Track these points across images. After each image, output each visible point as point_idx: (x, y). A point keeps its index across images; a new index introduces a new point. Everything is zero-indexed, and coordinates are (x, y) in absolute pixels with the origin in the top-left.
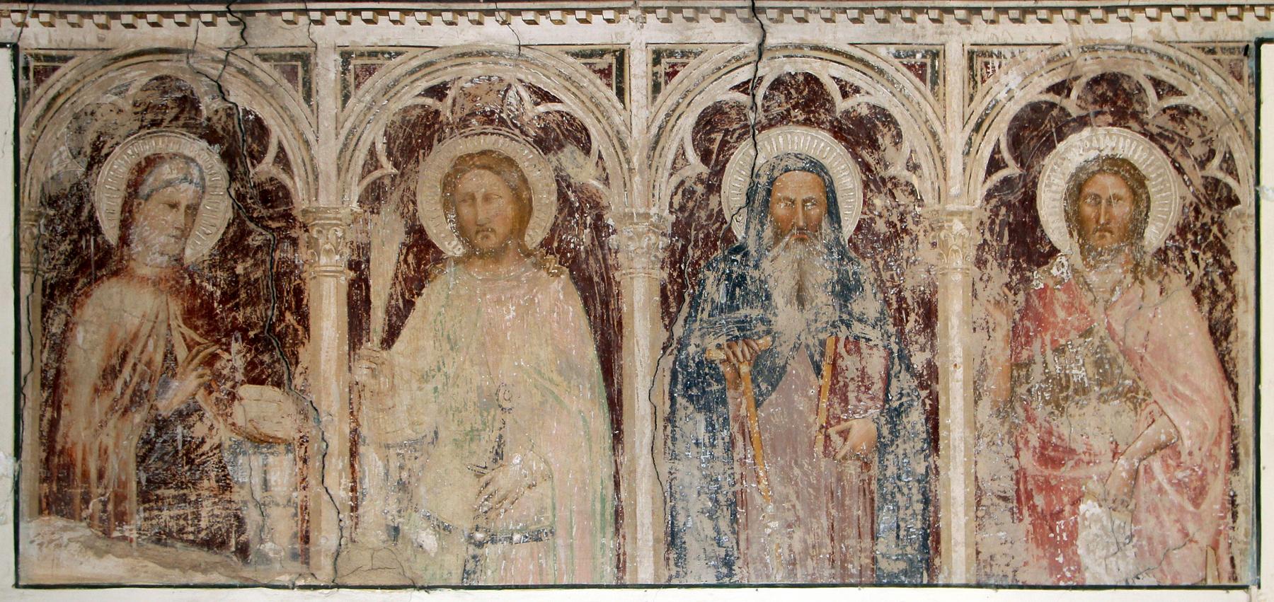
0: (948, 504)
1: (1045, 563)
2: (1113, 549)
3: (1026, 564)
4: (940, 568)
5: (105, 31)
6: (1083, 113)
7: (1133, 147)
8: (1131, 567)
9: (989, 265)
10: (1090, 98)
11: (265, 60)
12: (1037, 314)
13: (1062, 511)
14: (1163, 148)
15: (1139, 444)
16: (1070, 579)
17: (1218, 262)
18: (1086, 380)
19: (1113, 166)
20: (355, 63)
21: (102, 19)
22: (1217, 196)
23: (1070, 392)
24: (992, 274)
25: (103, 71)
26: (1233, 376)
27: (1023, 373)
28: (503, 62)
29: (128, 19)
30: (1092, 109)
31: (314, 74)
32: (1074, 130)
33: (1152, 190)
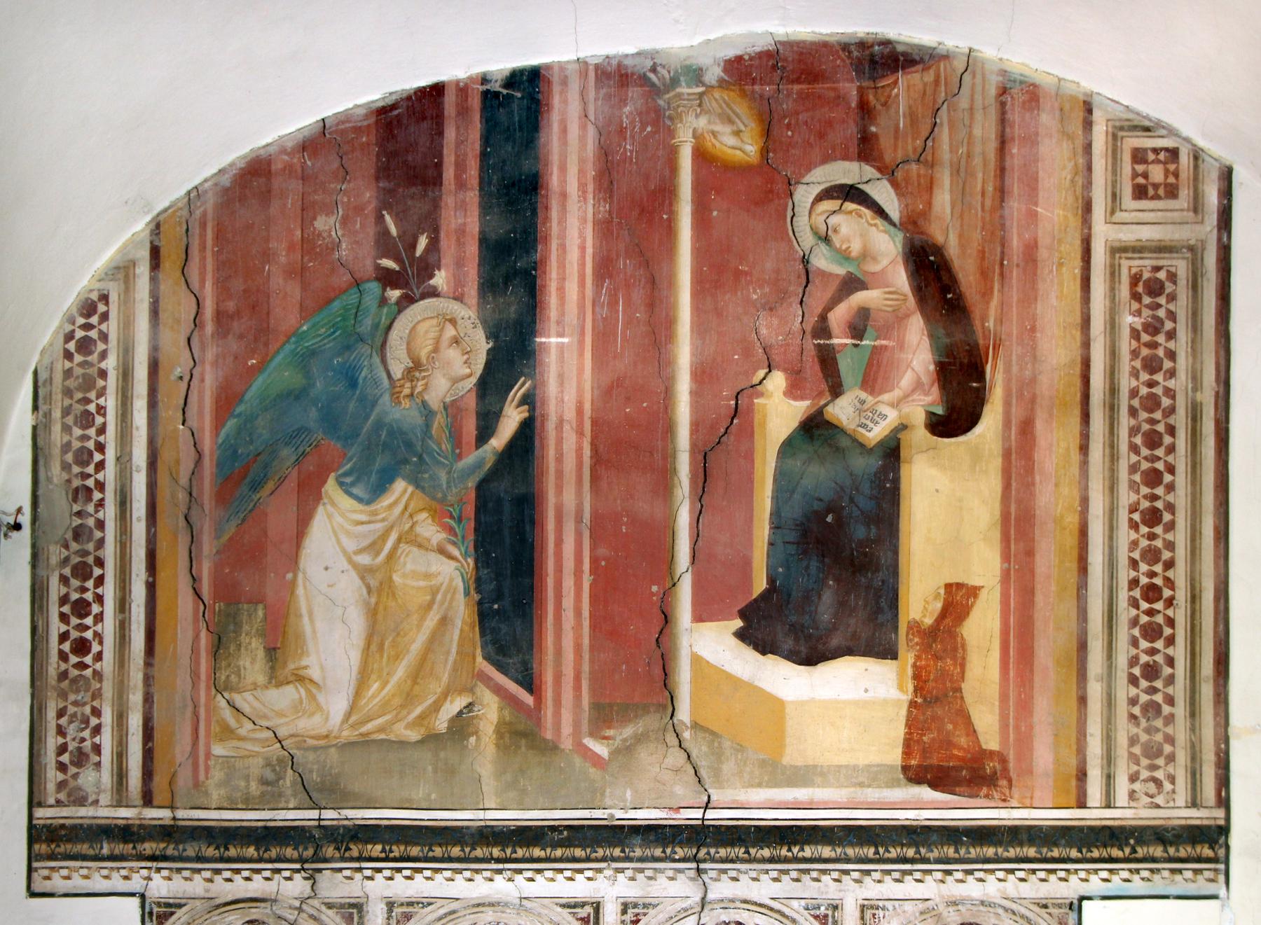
5: (210, 884)
11: (330, 908)
20: (398, 911)
21: (207, 874)
25: (207, 916)
28: (508, 911)
29: (227, 874)
31: (366, 920)
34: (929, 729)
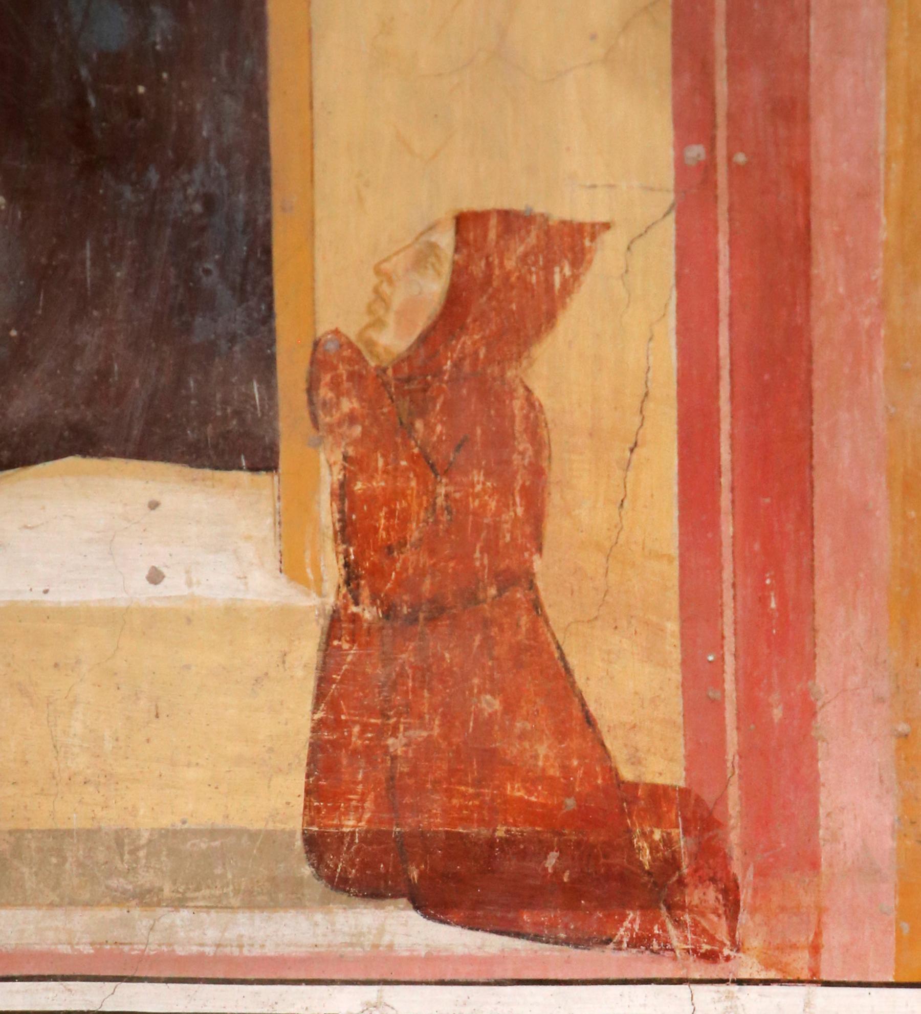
34: (409, 710)
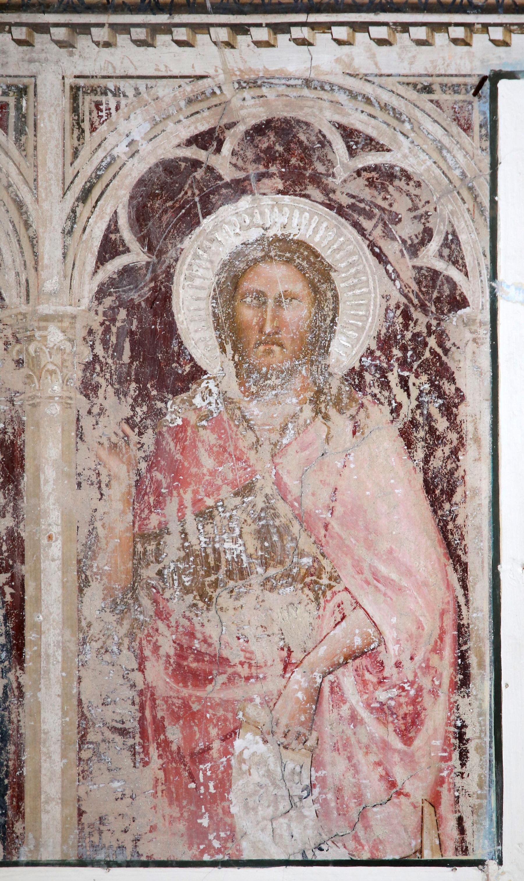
0: (37, 742)
1: (181, 827)
2: (283, 806)
3: (153, 829)
4: (22, 837)
6: (241, 175)
7: (313, 225)
8: (310, 832)
9: (101, 393)
10: (250, 154)
12: (172, 461)
13: (208, 749)
14: (356, 225)
15: (322, 650)
16: (219, 851)
17: (436, 388)
18: (244, 558)
19: (285, 251)
22: (435, 295)
23: (221, 575)
24: (106, 404)
26: (460, 553)
27: (151, 547)
30: (253, 170)
32: (227, 200)
33: (341, 285)
